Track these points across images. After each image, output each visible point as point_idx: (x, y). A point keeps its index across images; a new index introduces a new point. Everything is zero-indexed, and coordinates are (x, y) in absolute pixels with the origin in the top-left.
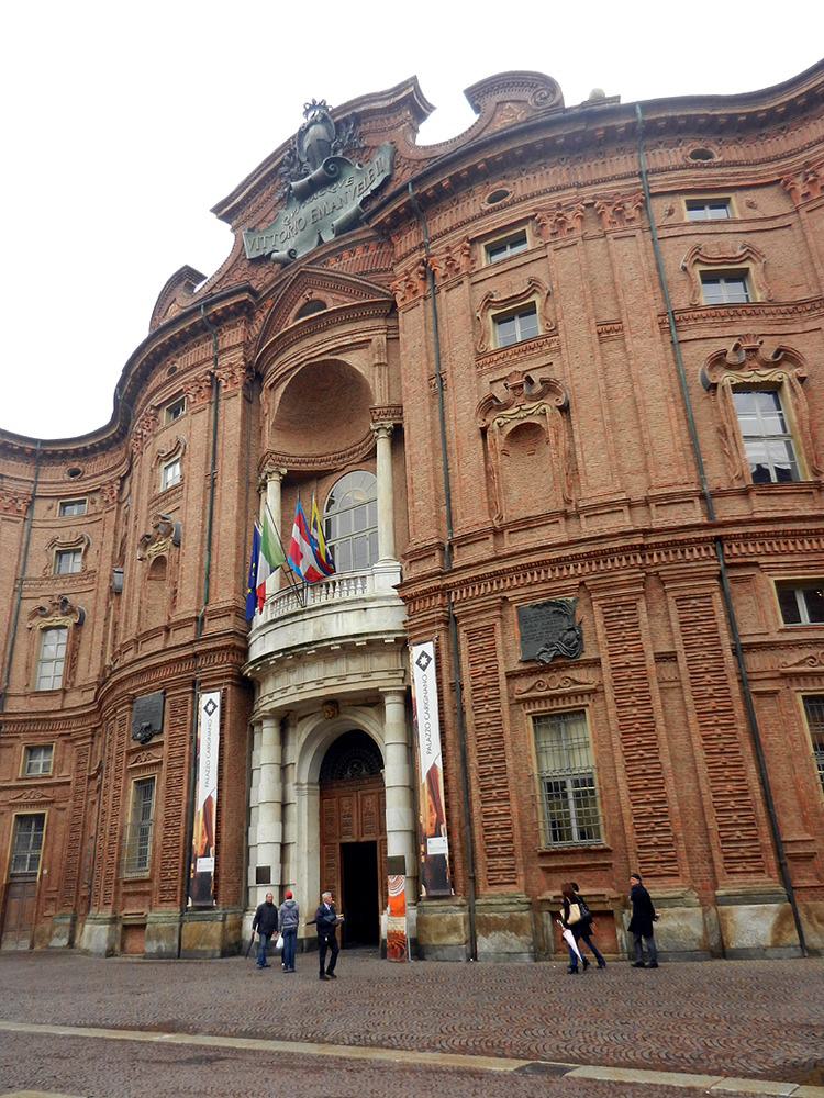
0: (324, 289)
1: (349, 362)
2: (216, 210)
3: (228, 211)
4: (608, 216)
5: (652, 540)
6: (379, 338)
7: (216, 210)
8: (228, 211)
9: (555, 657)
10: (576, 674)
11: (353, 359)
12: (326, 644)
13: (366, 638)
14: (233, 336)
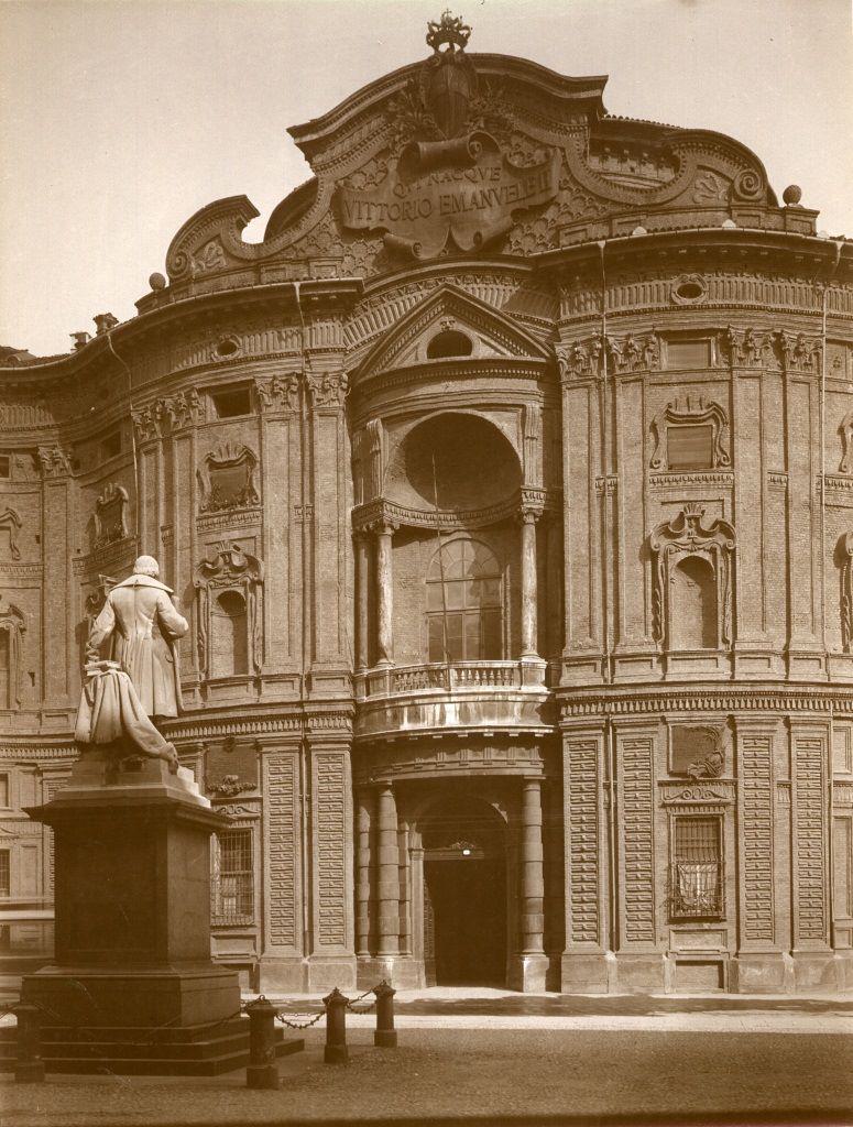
0: (468, 323)
1: (499, 425)
2: (295, 132)
3: (311, 138)
4: (790, 357)
5: (791, 689)
6: (535, 407)
7: (295, 132)
8: (311, 138)
9: (702, 775)
10: (713, 789)
11: (506, 424)
12: (480, 731)
13: (520, 730)
14: (327, 332)
